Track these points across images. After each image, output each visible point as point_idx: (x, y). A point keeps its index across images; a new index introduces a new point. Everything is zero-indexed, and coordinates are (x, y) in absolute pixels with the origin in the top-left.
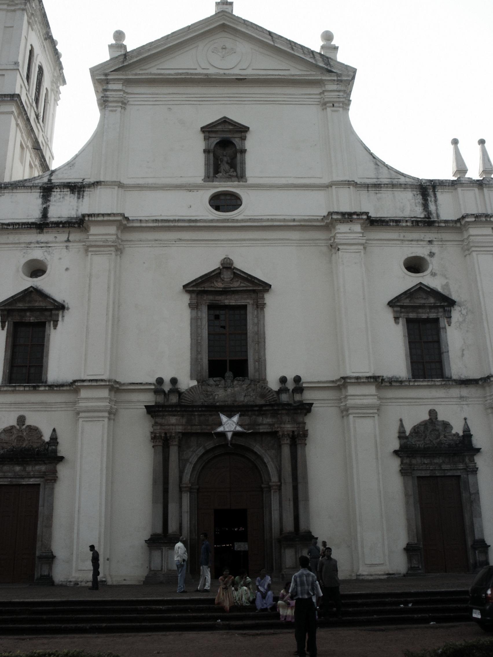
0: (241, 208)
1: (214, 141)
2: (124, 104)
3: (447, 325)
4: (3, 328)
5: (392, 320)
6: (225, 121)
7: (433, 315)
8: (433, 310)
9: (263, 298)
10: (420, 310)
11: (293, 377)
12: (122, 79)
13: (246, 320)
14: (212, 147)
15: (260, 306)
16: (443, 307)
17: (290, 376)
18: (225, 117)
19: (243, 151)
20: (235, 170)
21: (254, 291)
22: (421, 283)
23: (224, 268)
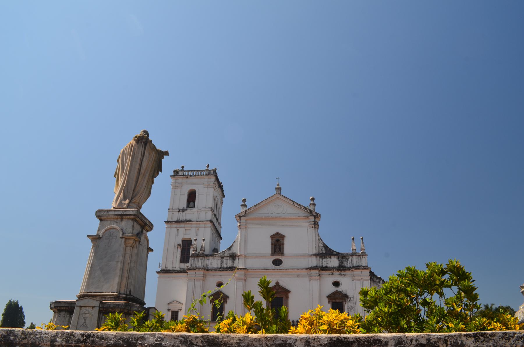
0: (282, 264)
1: (274, 240)
2: (246, 228)
3: (345, 304)
4: (211, 303)
5: (328, 302)
6: (277, 234)
7: (341, 301)
8: (341, 299)
9: (288, 295)
10: (337, 299)
11: (296, 320)
12: (245, 219)
13: (283, 301)
14: (274, 243)
15: (287, 297)
16: (344, 298)
17: (295, 321)
18: (278, 232)
19: (283, 244)
20: (281, 252)
21: (285, 293)
22: (337, 290)
23: (276, 285)
